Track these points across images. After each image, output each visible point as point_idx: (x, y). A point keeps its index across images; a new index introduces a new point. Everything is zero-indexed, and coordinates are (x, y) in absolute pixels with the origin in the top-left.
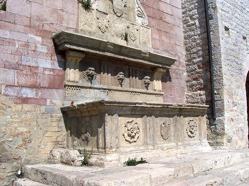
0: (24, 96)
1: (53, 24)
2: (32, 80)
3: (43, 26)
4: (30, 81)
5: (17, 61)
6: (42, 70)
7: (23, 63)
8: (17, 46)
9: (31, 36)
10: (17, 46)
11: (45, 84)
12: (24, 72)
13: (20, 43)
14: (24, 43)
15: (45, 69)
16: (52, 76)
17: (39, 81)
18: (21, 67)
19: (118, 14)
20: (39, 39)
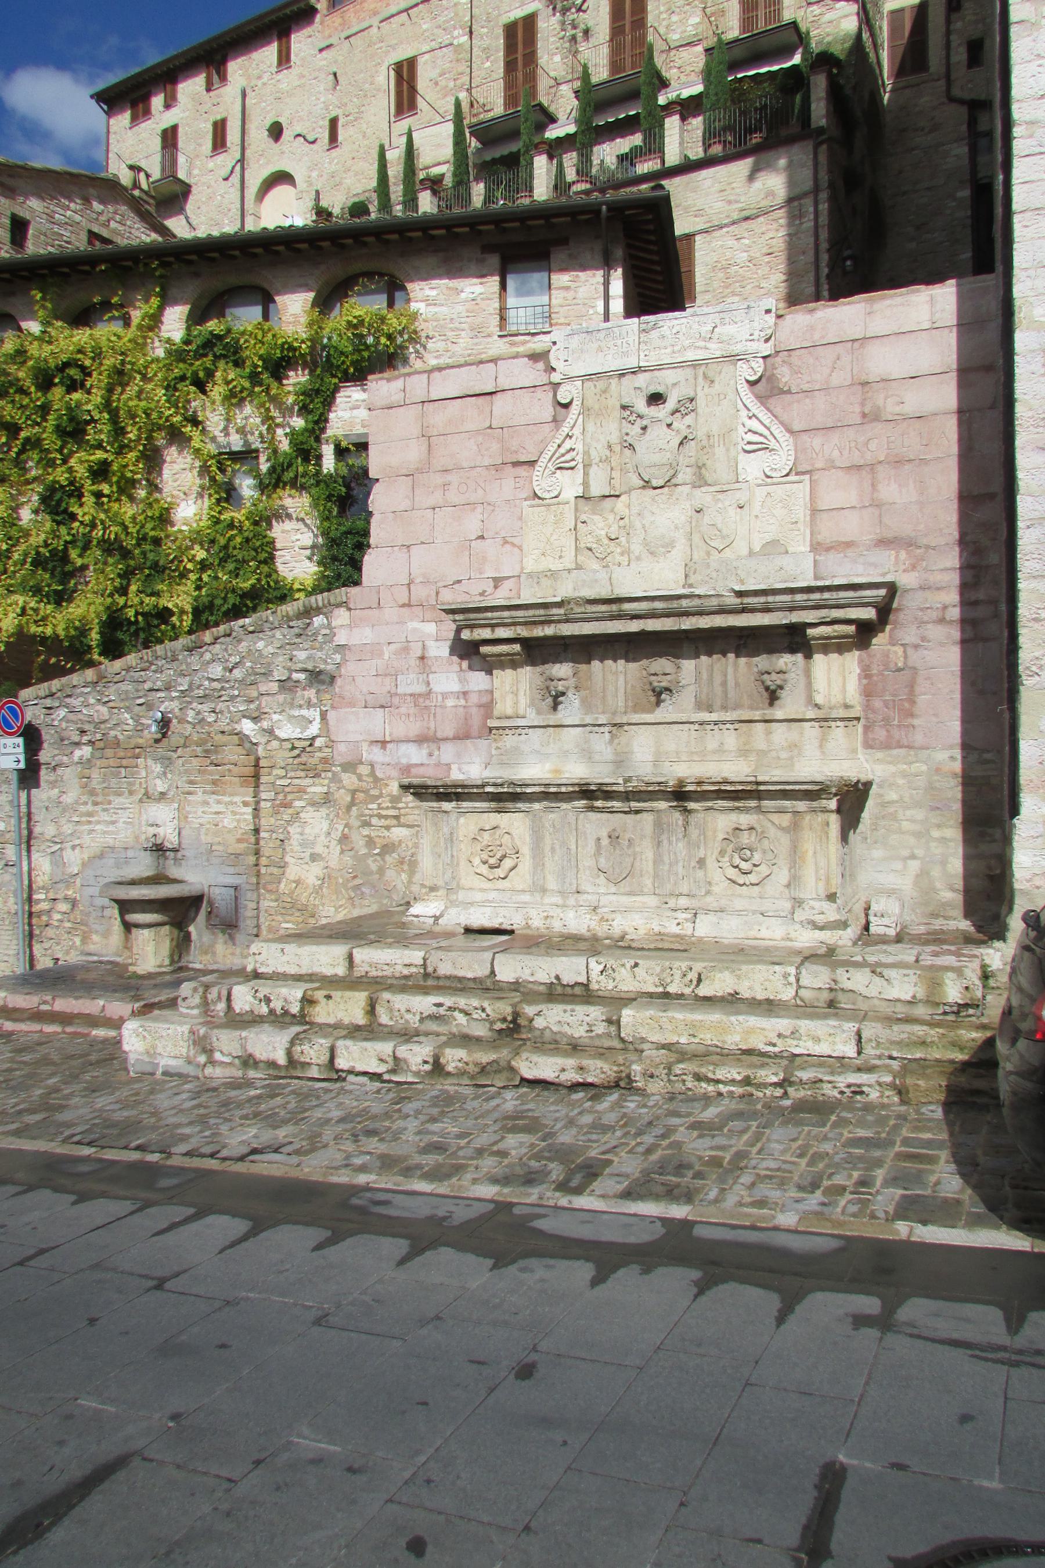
0: (404, 761)
1: (459, 582)
2: (419, 724)
3: (437, 593)
4: (414, 728)
5: (388, 688)
6: (440, 698)
7: (400, 691)
8: (386, 657)
9: (415, 624)
10: (386, 657)
11: (448, 730)
12: (403, 710)
13: (393, 647)
14: (398, 645)
15: (445, 696)
16: (461, 709)
17: (432, 725)
18: (396, 700)
19: (655, 483)
20: (431, 628)
